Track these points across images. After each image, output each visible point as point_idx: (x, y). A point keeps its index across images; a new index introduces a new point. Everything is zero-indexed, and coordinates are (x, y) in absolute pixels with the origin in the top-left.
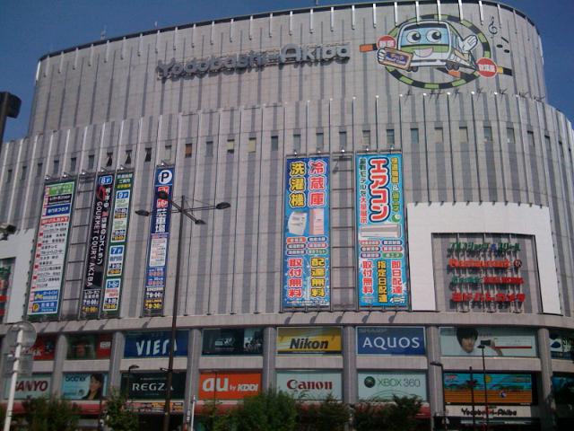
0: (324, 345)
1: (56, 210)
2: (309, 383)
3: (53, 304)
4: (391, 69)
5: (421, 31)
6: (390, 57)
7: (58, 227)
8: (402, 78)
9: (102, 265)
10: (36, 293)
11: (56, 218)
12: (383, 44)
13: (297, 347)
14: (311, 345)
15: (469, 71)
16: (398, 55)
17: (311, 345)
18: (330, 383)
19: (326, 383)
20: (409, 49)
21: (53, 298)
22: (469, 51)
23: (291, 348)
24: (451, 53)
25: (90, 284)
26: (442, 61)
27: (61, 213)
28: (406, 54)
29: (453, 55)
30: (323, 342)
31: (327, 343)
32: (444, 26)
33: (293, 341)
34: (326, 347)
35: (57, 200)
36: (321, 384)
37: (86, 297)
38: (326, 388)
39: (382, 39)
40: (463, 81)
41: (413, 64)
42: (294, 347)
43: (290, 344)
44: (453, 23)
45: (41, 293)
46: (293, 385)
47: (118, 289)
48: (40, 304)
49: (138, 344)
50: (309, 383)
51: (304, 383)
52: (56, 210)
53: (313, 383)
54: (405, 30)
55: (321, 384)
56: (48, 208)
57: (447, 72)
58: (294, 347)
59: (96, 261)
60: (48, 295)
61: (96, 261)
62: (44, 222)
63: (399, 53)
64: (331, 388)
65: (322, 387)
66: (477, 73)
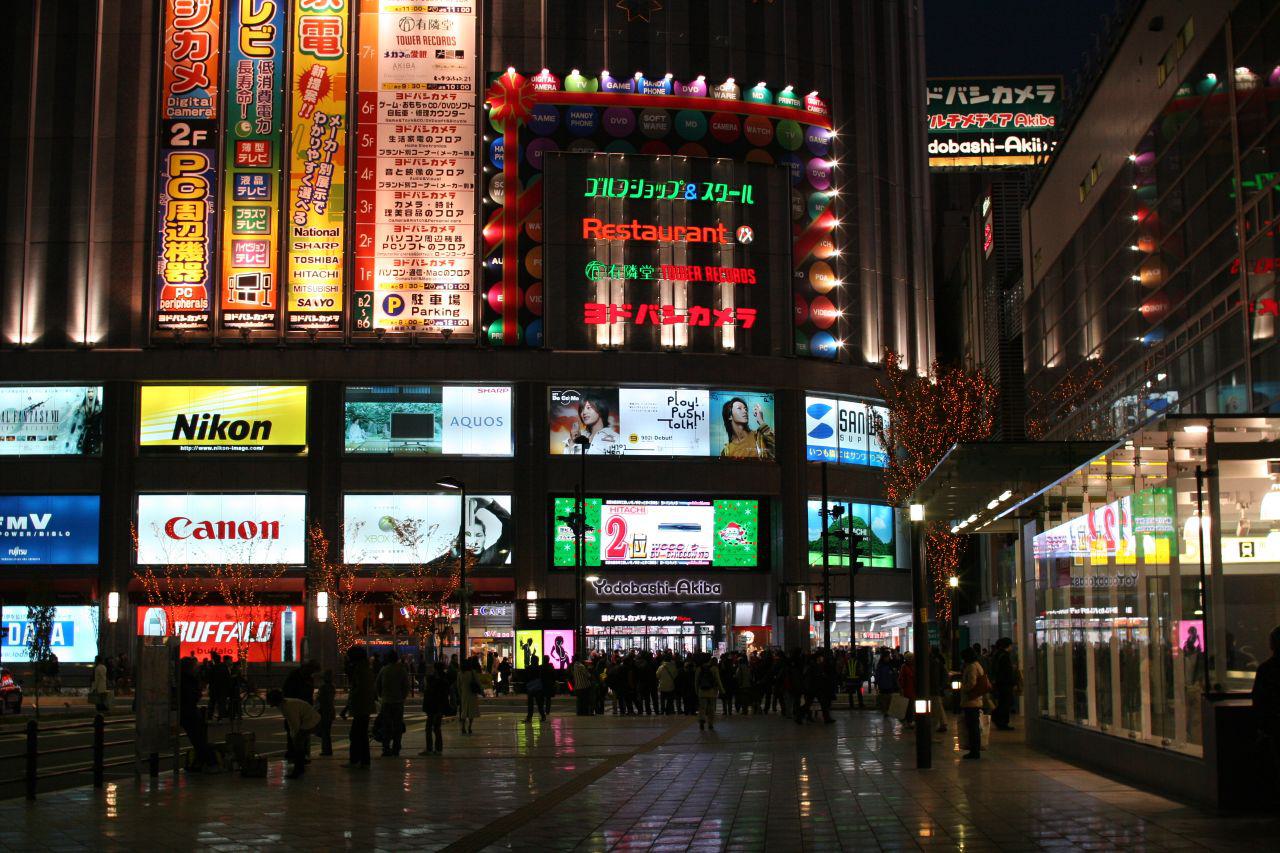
0: (261, 430)
2: (221, 525)
13: (190, 436)
14: (226, 430)
17: (226, 430)
18: (275, 525)
19: (265, 525)
23: (176, 436)
30: (257, 424)
31: (267, 425)
33: (181, 419)
34: (266, 436)
36: (252, 525)
38: (265, 535)
42: (182, 434)
43: (173, 427)
46: (178, 528)
50: (221, 525)
51: (208, 524)
53: (232, 524)
55: (252, 525)
58: (182, 434)
64: (275, 535)
65: (254, 532)
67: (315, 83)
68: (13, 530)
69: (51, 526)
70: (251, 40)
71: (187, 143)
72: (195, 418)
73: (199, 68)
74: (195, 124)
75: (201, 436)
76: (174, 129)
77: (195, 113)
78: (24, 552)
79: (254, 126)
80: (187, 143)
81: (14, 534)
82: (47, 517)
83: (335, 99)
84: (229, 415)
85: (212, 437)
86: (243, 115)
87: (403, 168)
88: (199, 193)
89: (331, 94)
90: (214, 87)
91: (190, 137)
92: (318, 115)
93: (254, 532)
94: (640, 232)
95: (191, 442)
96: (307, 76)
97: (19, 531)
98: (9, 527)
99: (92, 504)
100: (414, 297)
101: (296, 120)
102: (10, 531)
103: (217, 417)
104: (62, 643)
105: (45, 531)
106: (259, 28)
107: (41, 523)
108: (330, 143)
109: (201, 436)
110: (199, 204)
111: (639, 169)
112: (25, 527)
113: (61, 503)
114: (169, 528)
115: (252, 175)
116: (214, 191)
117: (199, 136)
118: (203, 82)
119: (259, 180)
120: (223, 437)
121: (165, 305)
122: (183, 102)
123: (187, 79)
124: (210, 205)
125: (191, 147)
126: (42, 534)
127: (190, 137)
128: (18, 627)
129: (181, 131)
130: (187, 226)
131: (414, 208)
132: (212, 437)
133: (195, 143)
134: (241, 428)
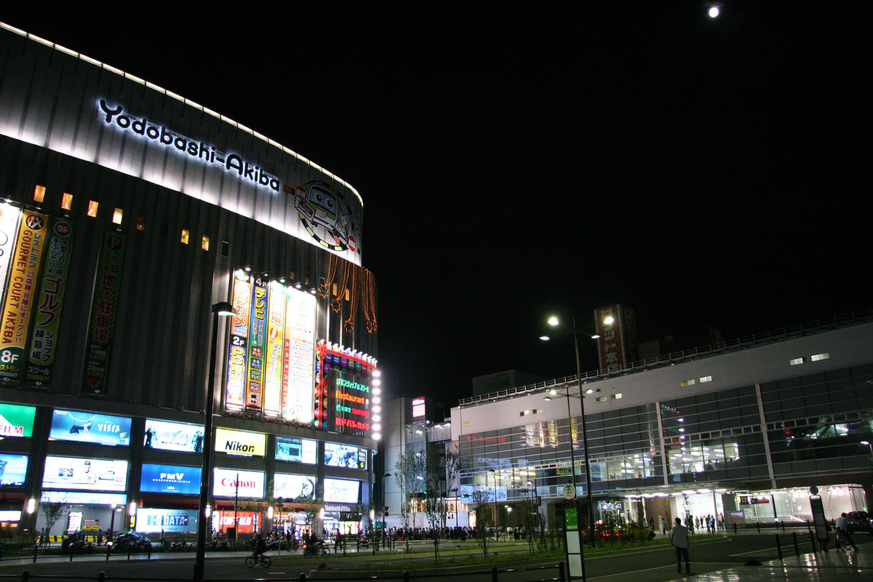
4: (303, 217)
5: (321, 194)
6: (302, 206)
8: (308, 228)
12: (298, 192)
14: (241, 448)
15: (344, 242)
16: (306, 206)
17: (241, 448)
20: (314, 206)
22: (346, 226)
23: (226, 449)
24: (336, 222)
26: (331, 226)
28: (312, 210)
29: (337, 225)
32: (334, 198)
33: (228, 443)
34: (253, 451)
38: (251, 486)
39: (299, 188)
40: (340, 248)
41: (315, 220)
44: (339, 199)
46: (225, 482)
54: (314, 188)
57: (333, 237)
63: (307, 205)
65: (248, 485)
66: (348, 246)
67: (274, 333)
68: (170, 479)
69: (183, 479)
70: (258, 313)
71: (238, 344)
72: (232, 443)
73: (242, 318)
74: (241, 338)
75: (234, 449)
76: (235, 338)
77: (241, 334)
78: (173, 488)
79: (258, 343)
80: (238, 344)
81: (170, 481)
82: (182, 475)
83: (280, 339)
84: (242, 443)
85: (237, 450)
86: (255, 338)
87: (296, 366)
88: (241, 363)
89: (278, 337)
90: (247, 326)
91: (239, 342)
92: (275, 344)
93: (248, 485)
94: (348, 397)
95: (230, 451)
96: (272, 330)
97: (172, 480)
98: (168, 478)
99: (199, 471)
100: (297, 409)
101: (269, 344)
102: (169, 479)
103: (238, 443)
104: (184, 524)
105: (181, 480)
106: (260, 309)
107: (180, 477)
108: (278, 353)
109: (234, 449)
110: (241, 366)
111: (346, 377)
112: (174, 478)
113: (188, 470)
114: (223, 482)
115: (256, 360)
116: (245, 363)
117: (242, 342)
118: (243, 324)
119: (258, 362)
120: (240, 450)
121: (229, 400)
122: (238, 330)
123: (239, 322)
124: (244, 367)
125: (239, 346)
126: (180, 481)
127: (239, 342)
128: (168, 517)
129: (236, 339)
130: (237, 373)
131: (298, 380)
132: (237, 450)
133: (241, 345)
134: (246, 448)
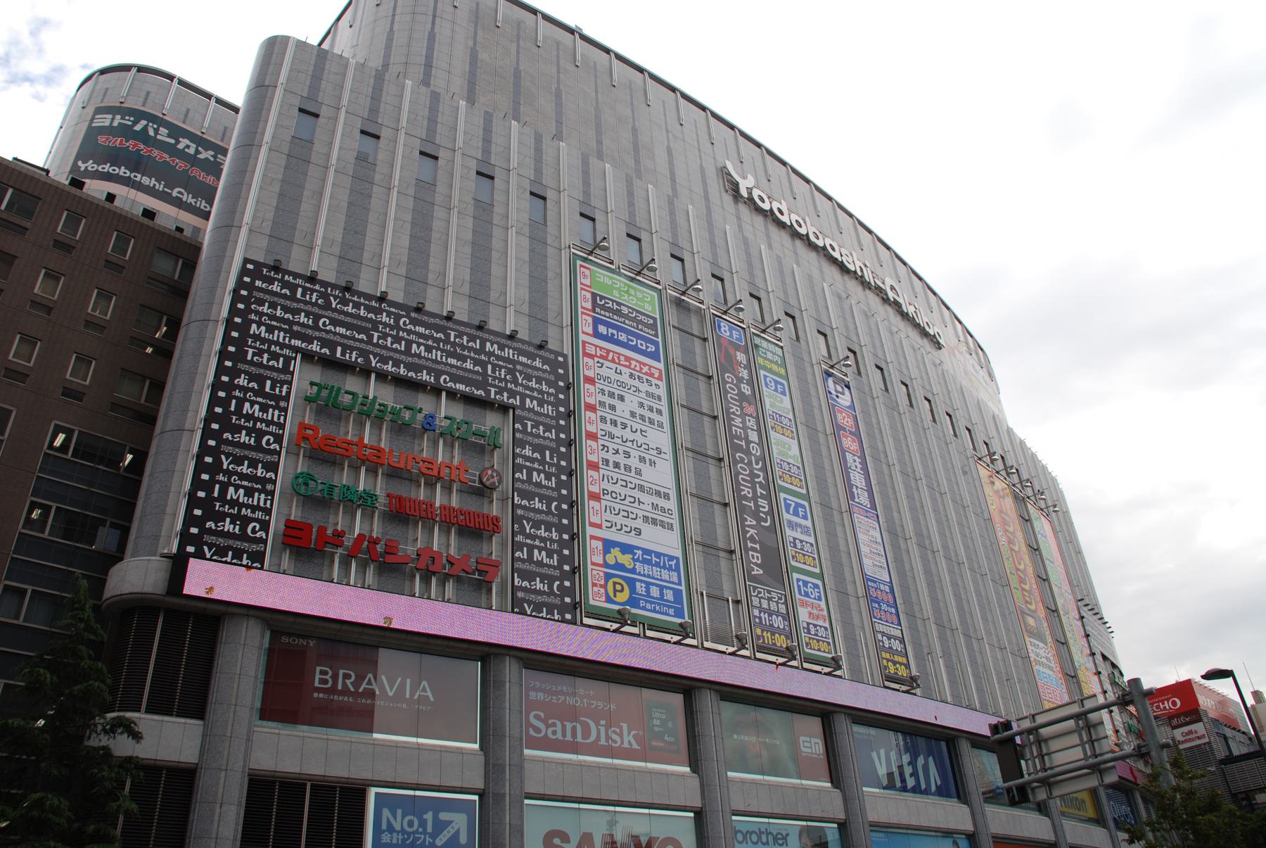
1: (623, 337)
3: (669, 595)
7: (630, 382)
9: (773, 528)
10: (608, 545)
11: (628, 359)
21: (665, 574)
25: (757, 571)
27: (635, 349)
35: (626, 316)
37: (756, 602)
45: (627, 549)
47: (823, 604)
48: (631, 583)
49: (874, 754)
52: (623, 337)
56: (596, 322)
59: (756, 514)
60: (645, 561)
61: (756, 514)
62: (591, 350)
